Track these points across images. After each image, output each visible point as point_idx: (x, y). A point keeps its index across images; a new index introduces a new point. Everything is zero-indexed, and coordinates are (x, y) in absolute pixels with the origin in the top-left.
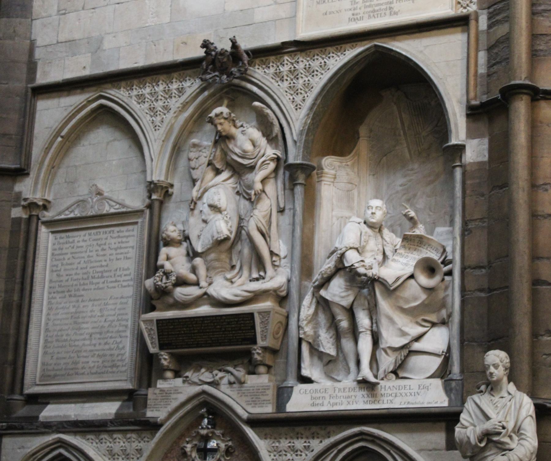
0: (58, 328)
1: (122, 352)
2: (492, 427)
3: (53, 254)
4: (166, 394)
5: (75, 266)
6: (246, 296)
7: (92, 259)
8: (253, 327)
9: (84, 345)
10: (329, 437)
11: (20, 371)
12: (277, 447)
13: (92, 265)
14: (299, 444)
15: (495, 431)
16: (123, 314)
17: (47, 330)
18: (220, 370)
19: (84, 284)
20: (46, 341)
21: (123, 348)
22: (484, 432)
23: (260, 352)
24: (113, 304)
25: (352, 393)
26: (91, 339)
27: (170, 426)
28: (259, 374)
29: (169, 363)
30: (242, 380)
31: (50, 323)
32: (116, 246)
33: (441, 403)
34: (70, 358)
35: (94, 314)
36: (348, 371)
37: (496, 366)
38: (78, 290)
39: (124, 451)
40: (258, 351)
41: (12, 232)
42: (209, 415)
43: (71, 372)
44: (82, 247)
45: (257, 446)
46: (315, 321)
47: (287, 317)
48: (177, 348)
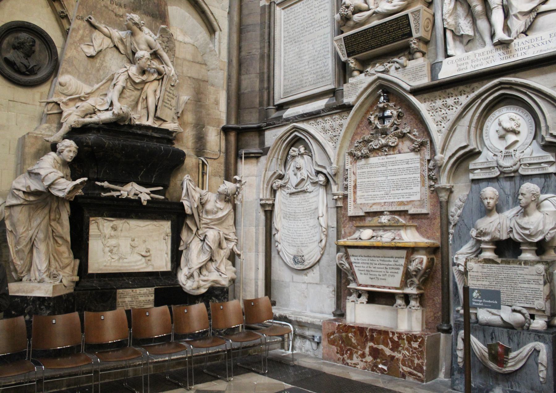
0: (290, 63)
1: (327, 68)
3: (284, 21)
4: (355, 85)
5: (296, 25)
6: (401, 5)
7: (305, 17)
8: (409, 25)
9: (305, 69)
10: (473, 92)
11: (272, 92)
12: (434, 106)
13: (306, 20)
14: (450, 101)
16: (326, 44)
17: (285, 66)
18: (389, 63)
19: (302, 33)
20: (285, 72)
21: (328, 65)
23: (416, 42)
24: (320, 40)
25: (490, 55)
26: (308, 65)
27: (358, 105)
28: (417, 58)
29: (355, 65)
30: (405, 64)
31: (286, 61)
32: (318, 5)
34: (298, 78)
35: (309, 49)
36: (484, 44)
38: (300, 37)
39: (332, 127)
40: (414, 41)
41: (261, 14)
42: (384, 94)
43: (299, 87)
44: (299, 12)
45: (419, 107)
46: (455, 14)
47: (434, 15)
48: (358, 54)
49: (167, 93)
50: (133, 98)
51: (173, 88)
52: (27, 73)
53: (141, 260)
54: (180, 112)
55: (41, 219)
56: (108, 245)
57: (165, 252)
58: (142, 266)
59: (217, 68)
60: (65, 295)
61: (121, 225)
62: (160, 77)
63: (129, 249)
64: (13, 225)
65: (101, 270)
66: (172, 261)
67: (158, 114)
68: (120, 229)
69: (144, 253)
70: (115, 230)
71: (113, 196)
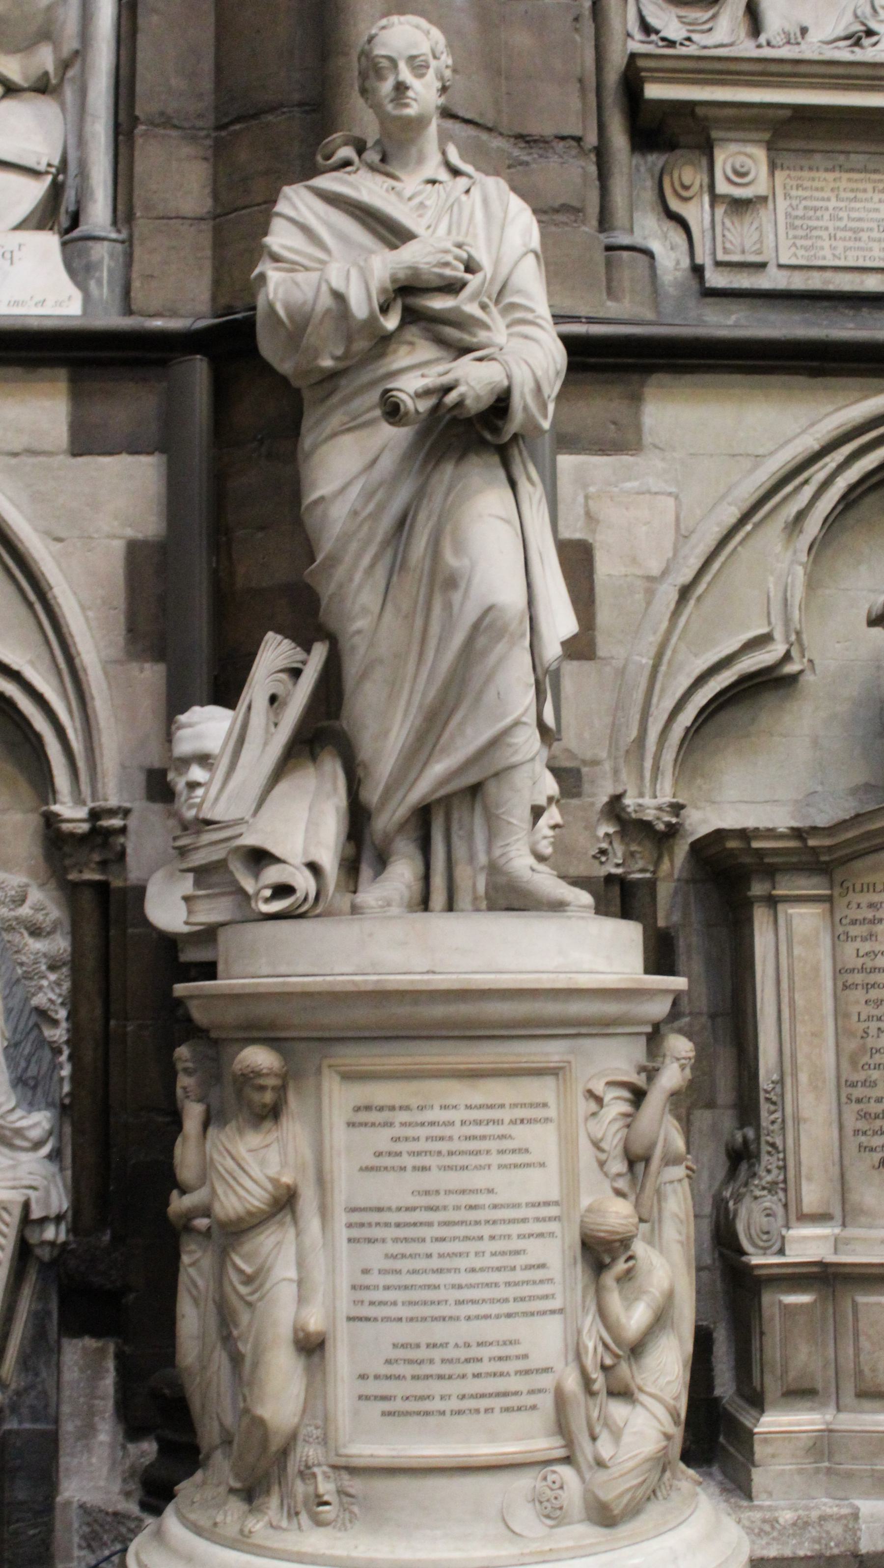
2: (432, 259)
15: (441, 276)
22: (401, 275)
33: (59, 303)
37: (418, 66)
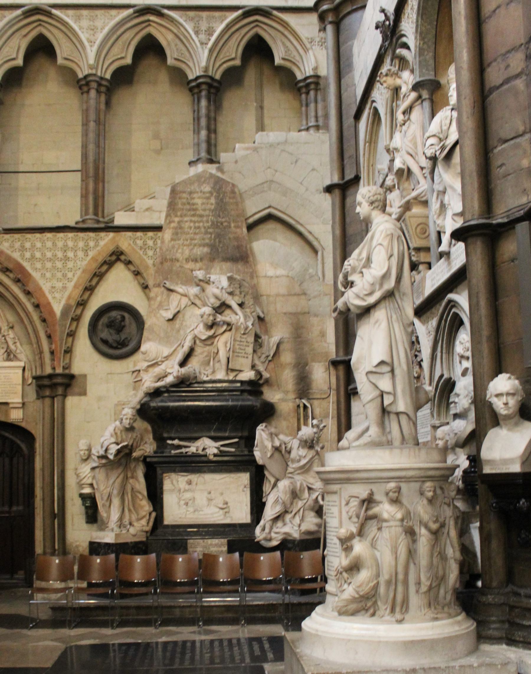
49: (238, 343)
50: (205, 354)
51: (245, 336)
52: (119, 346)
53: (219, 512)
54: (272, 355)
55: (115, 479)
56: (183, 498)
57: (245, 504)
58: (219, 518)
59: (320, 295)
60: (131, 543)
61: (196, 479)
62: (229, 328)
63: (205, 502)
64: (97, 483)
65: (176, 521)
66: (252, 513)
67: (230, 366)
68: (195, 483)
69: (221, 506)
70: (190, 484)
71: (182, 453)
